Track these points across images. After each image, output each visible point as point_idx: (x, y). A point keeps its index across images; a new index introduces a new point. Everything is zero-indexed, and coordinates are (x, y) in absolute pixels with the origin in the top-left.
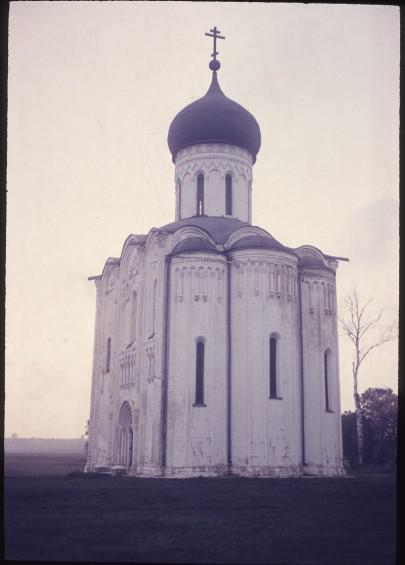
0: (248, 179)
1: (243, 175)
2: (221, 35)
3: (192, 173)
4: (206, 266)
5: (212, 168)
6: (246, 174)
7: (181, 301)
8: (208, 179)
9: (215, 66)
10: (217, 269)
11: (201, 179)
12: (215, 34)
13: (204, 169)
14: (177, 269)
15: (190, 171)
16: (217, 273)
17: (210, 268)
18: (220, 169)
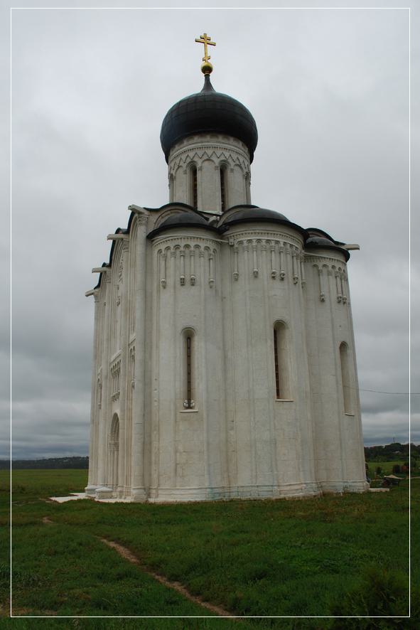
0: (245, 170)
1: (240, 166)
2: (212, 41)
3: (185, 166)
5: (205, 157)
6: (243, 166)
7: (164, 287)
8: (201, 169)
9: (207, 70)
11: (194, 171)
12: (205, 40)
13: (196, 159)
14: (160, 251)
15: (182, 164)
16: (206, 253)
18: (214, 158)
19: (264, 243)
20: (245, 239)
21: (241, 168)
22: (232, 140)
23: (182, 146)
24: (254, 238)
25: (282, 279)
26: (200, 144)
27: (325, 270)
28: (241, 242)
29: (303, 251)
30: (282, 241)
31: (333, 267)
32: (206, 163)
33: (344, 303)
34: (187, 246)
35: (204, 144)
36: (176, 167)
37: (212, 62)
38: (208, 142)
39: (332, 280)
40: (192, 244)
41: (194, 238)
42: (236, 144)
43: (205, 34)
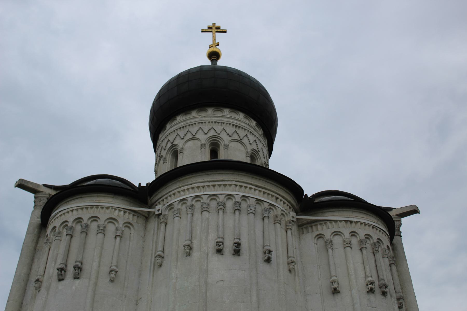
0: (249, 148)
1: (240, 141)
4: (85, 215)
5: (189, 136)
6: (245, 141)
9: (214, 56)
10: (112, 220)
13: (176, 142)
17: (95, 218)
18: (201, 136)
19: (205, 199)
20: (174, 200)
21: (242, 144)
22: (226, 112)
23: (165, 131)
24: (189, 195)
25: (237, 252)
26: (184, 123)
27: (337, 240)
28: (171, 206)
29: (293, 214)
30: (238, 193)
31: (353, 234)
32: (191, 143)
33: (384, 294)
34: (79, 220)
35: (187, 122)
36: (159, 158)
37: (221, 49)
38: (194, 118)
39: (355, 256)
40: (85, 215)
41: (92, 207)
42: (233, 115)
43: (214, 24)
